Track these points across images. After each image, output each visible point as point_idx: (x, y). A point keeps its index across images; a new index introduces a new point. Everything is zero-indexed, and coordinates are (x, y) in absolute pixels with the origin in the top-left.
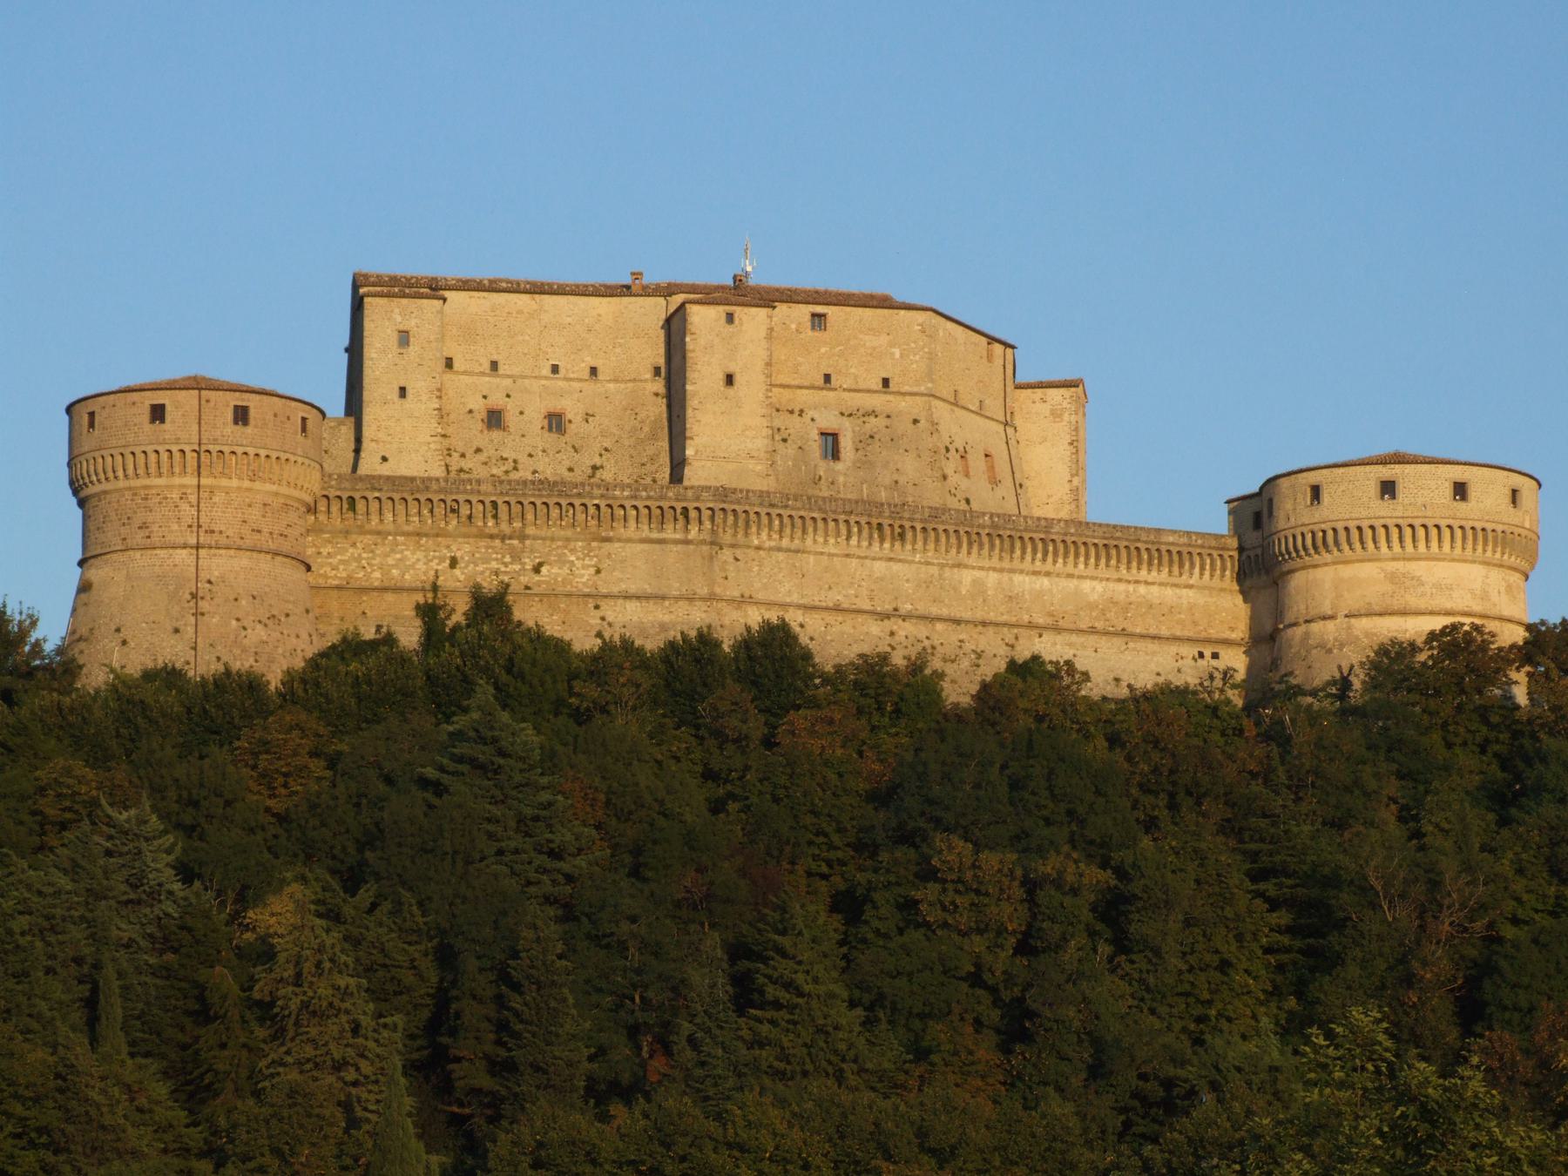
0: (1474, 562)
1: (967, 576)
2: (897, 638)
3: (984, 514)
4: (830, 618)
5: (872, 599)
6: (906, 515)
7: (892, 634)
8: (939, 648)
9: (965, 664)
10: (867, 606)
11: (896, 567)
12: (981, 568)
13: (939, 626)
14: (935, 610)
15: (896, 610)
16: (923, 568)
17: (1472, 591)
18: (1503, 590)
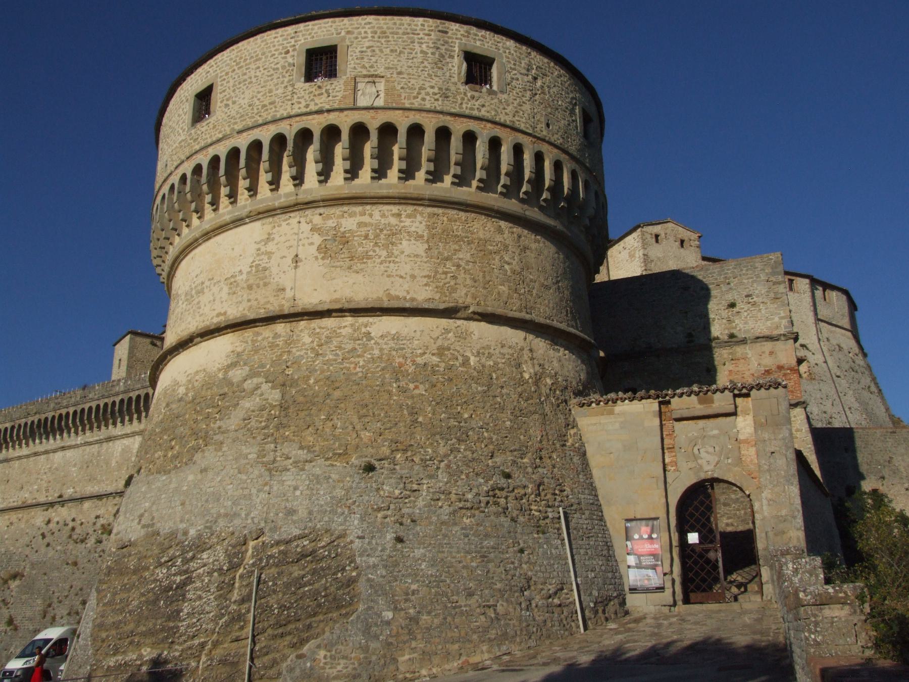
0: (238, 222)
1: (118, 446)
2: (51, 525)
3: (119, 380)
4: (14, 516)
5: (47, 491)
6: (65, 403)
7: (49, 522)
8: (78, 531)
9: (91, 541)
10: (42, 499)
11: (69, 453)
12: (127, 436)
13: (87, 505)
14: (91, 489)
15: (60, 496)
16: (88, 448)
17: (231, 282)
18: (308, 251)
